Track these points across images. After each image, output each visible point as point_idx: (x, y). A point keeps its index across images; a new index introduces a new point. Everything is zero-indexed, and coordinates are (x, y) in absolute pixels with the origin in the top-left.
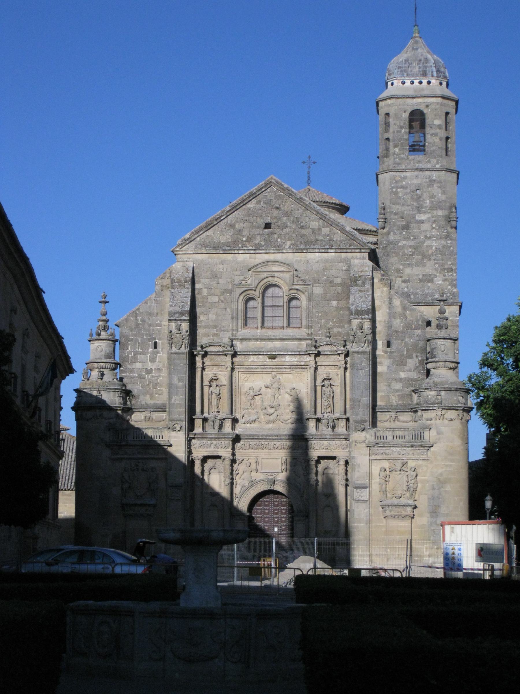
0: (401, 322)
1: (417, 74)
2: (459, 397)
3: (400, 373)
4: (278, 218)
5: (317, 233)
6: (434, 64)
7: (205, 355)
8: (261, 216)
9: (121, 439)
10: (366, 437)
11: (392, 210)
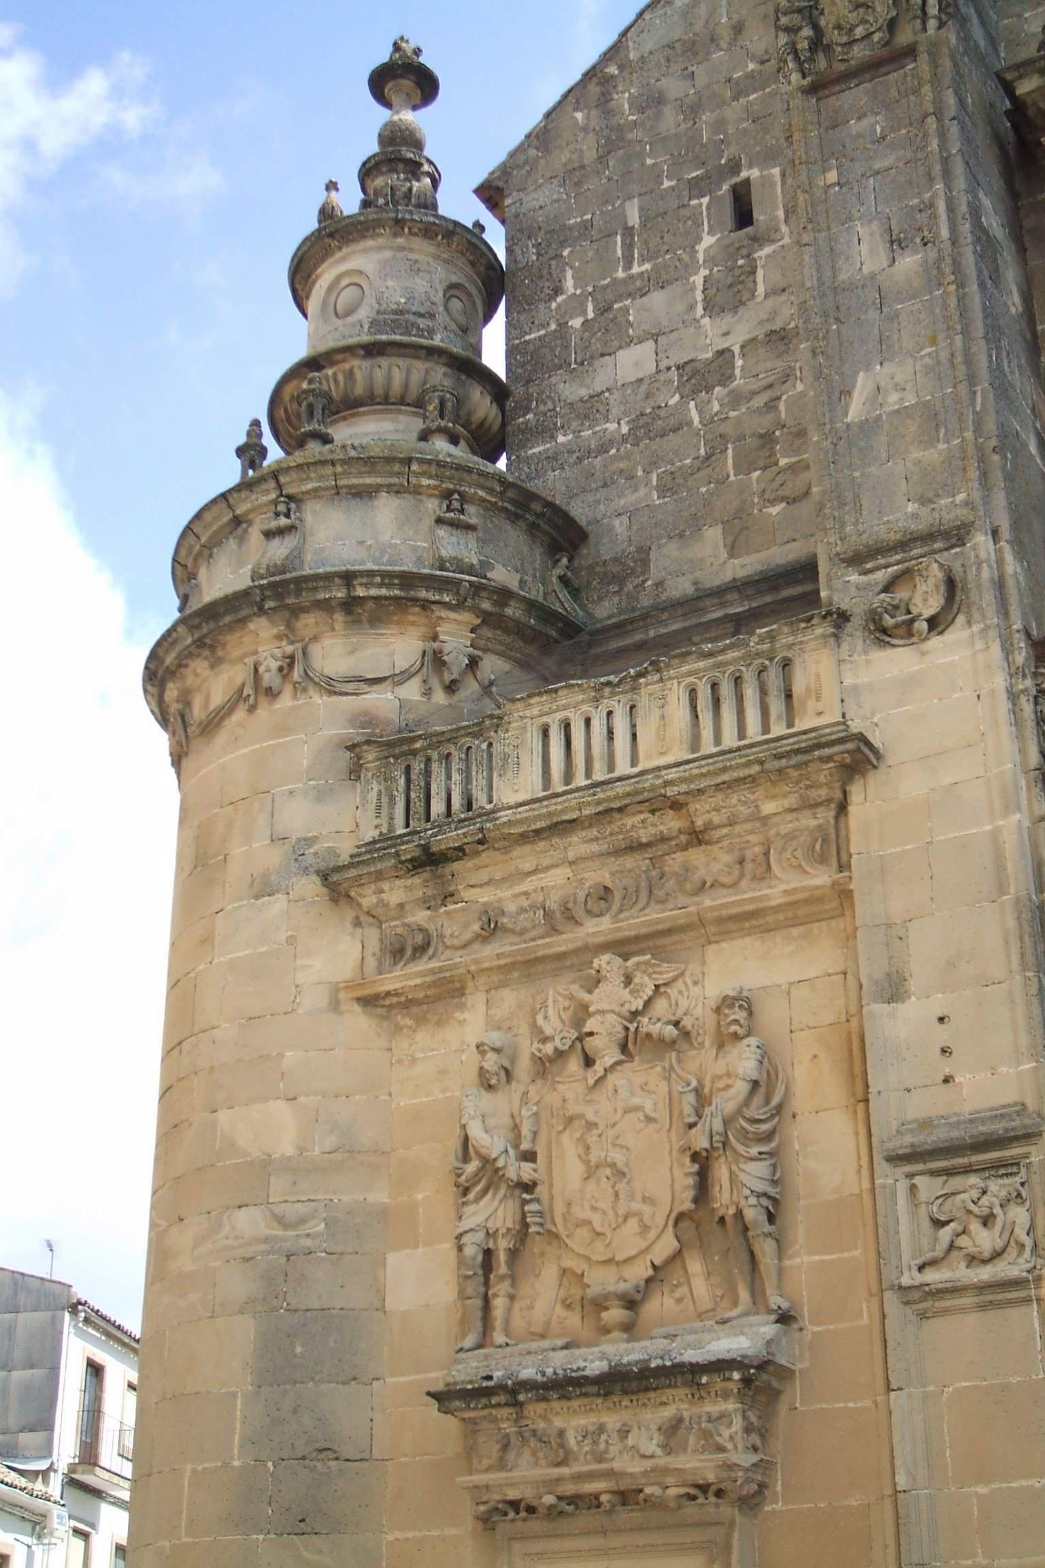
9: (449, 813)
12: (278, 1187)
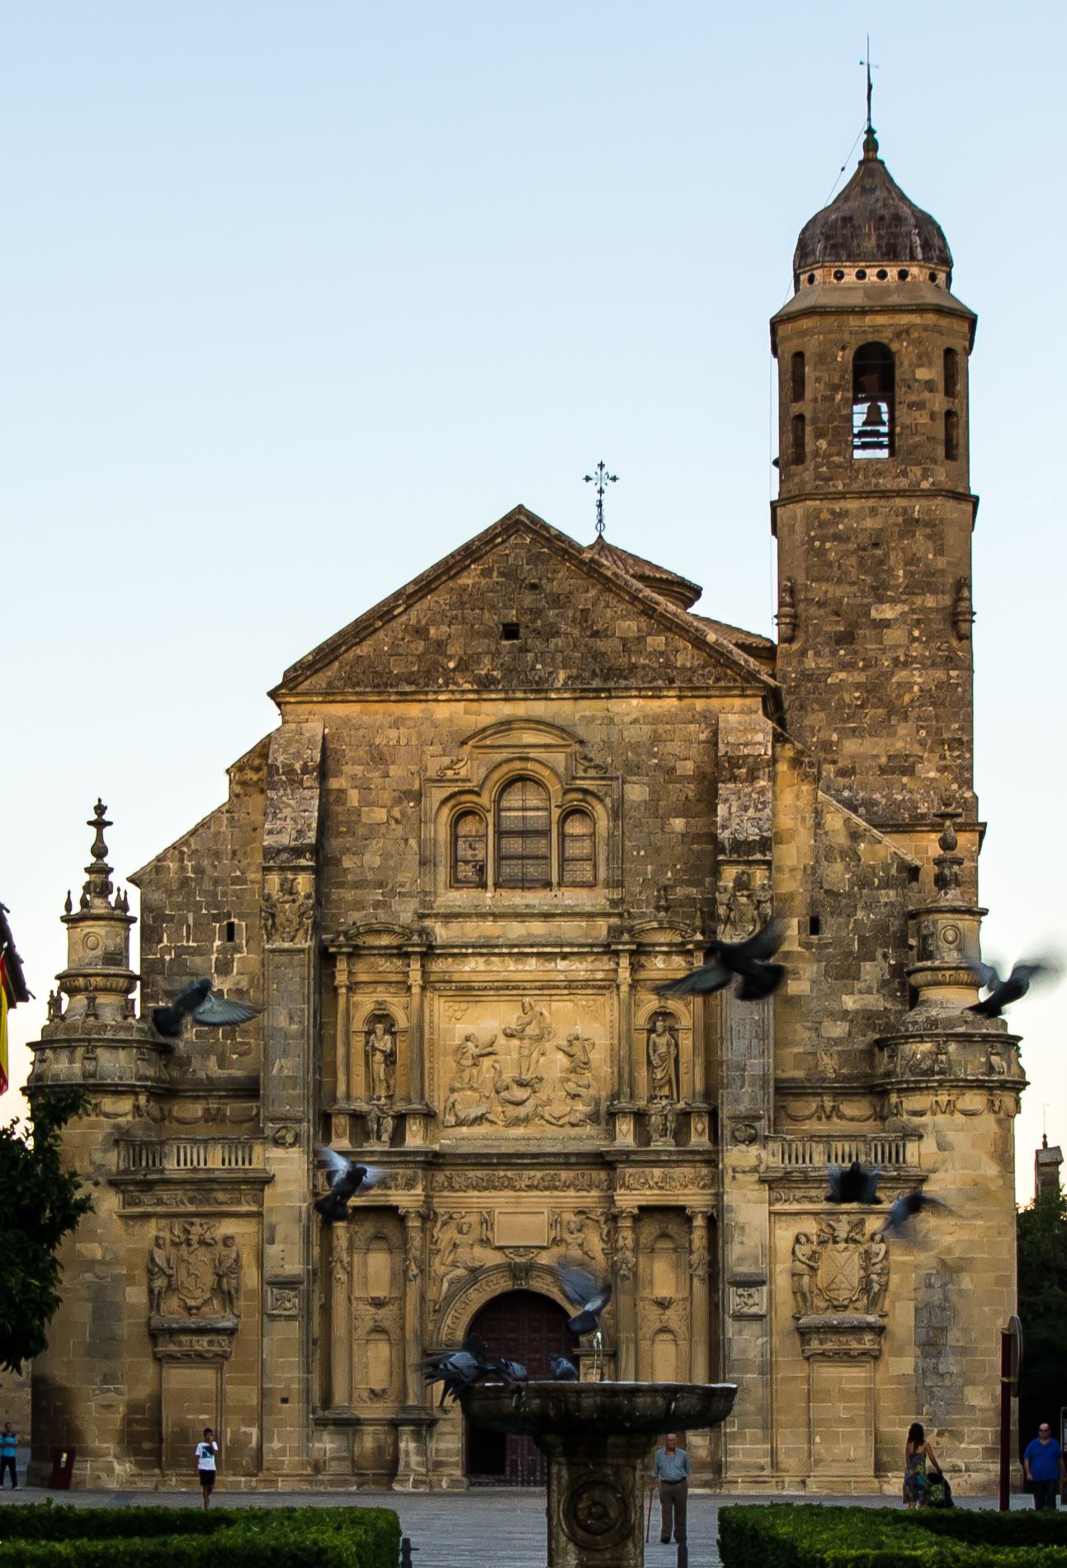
0: (847, 868)
1: (873, 255)
2: (993, 1058)
4: (537, 613)
6: (916, 227)
7: (355, 954)
8: (493, 607)
10: (759, 1157)
11: (810, 596)
12: (97, 1269)
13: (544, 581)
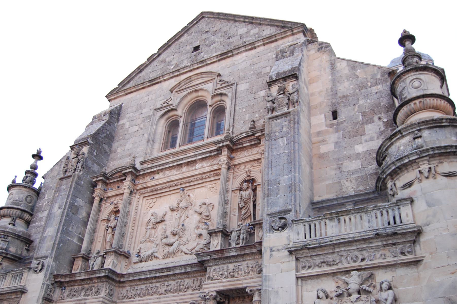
3: (356, 146)
5: (244, 36)
13: (211, 28)
